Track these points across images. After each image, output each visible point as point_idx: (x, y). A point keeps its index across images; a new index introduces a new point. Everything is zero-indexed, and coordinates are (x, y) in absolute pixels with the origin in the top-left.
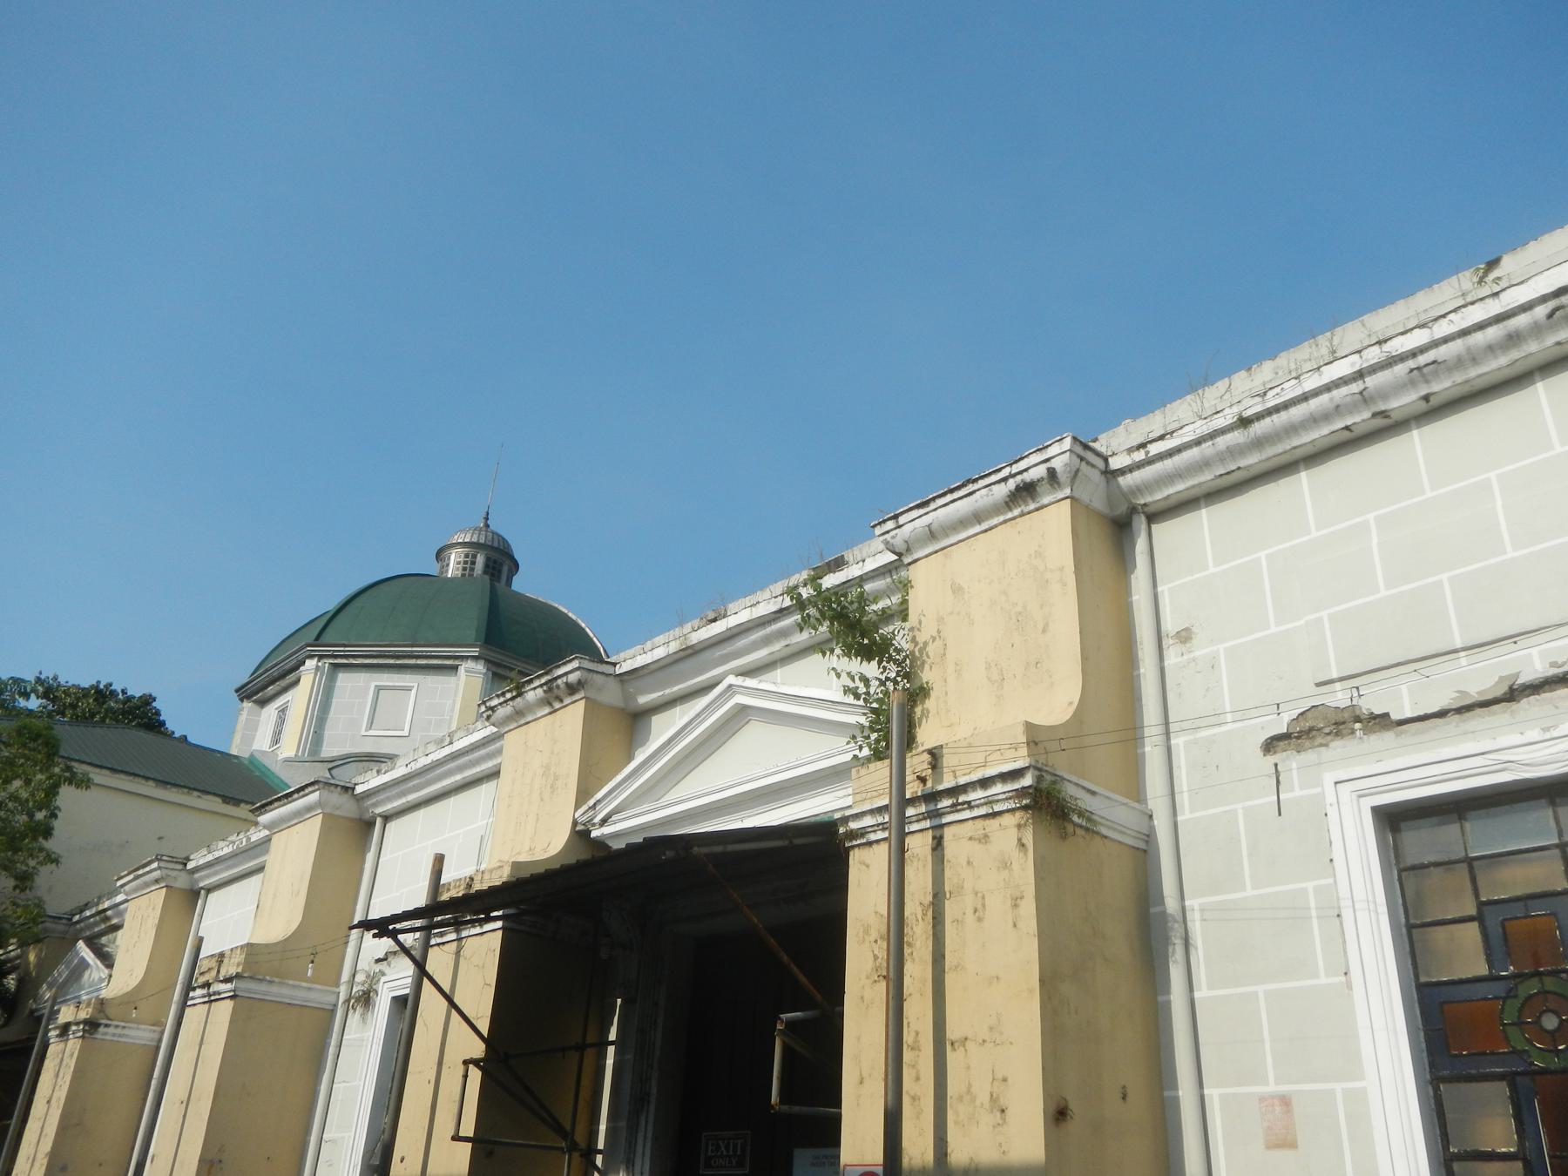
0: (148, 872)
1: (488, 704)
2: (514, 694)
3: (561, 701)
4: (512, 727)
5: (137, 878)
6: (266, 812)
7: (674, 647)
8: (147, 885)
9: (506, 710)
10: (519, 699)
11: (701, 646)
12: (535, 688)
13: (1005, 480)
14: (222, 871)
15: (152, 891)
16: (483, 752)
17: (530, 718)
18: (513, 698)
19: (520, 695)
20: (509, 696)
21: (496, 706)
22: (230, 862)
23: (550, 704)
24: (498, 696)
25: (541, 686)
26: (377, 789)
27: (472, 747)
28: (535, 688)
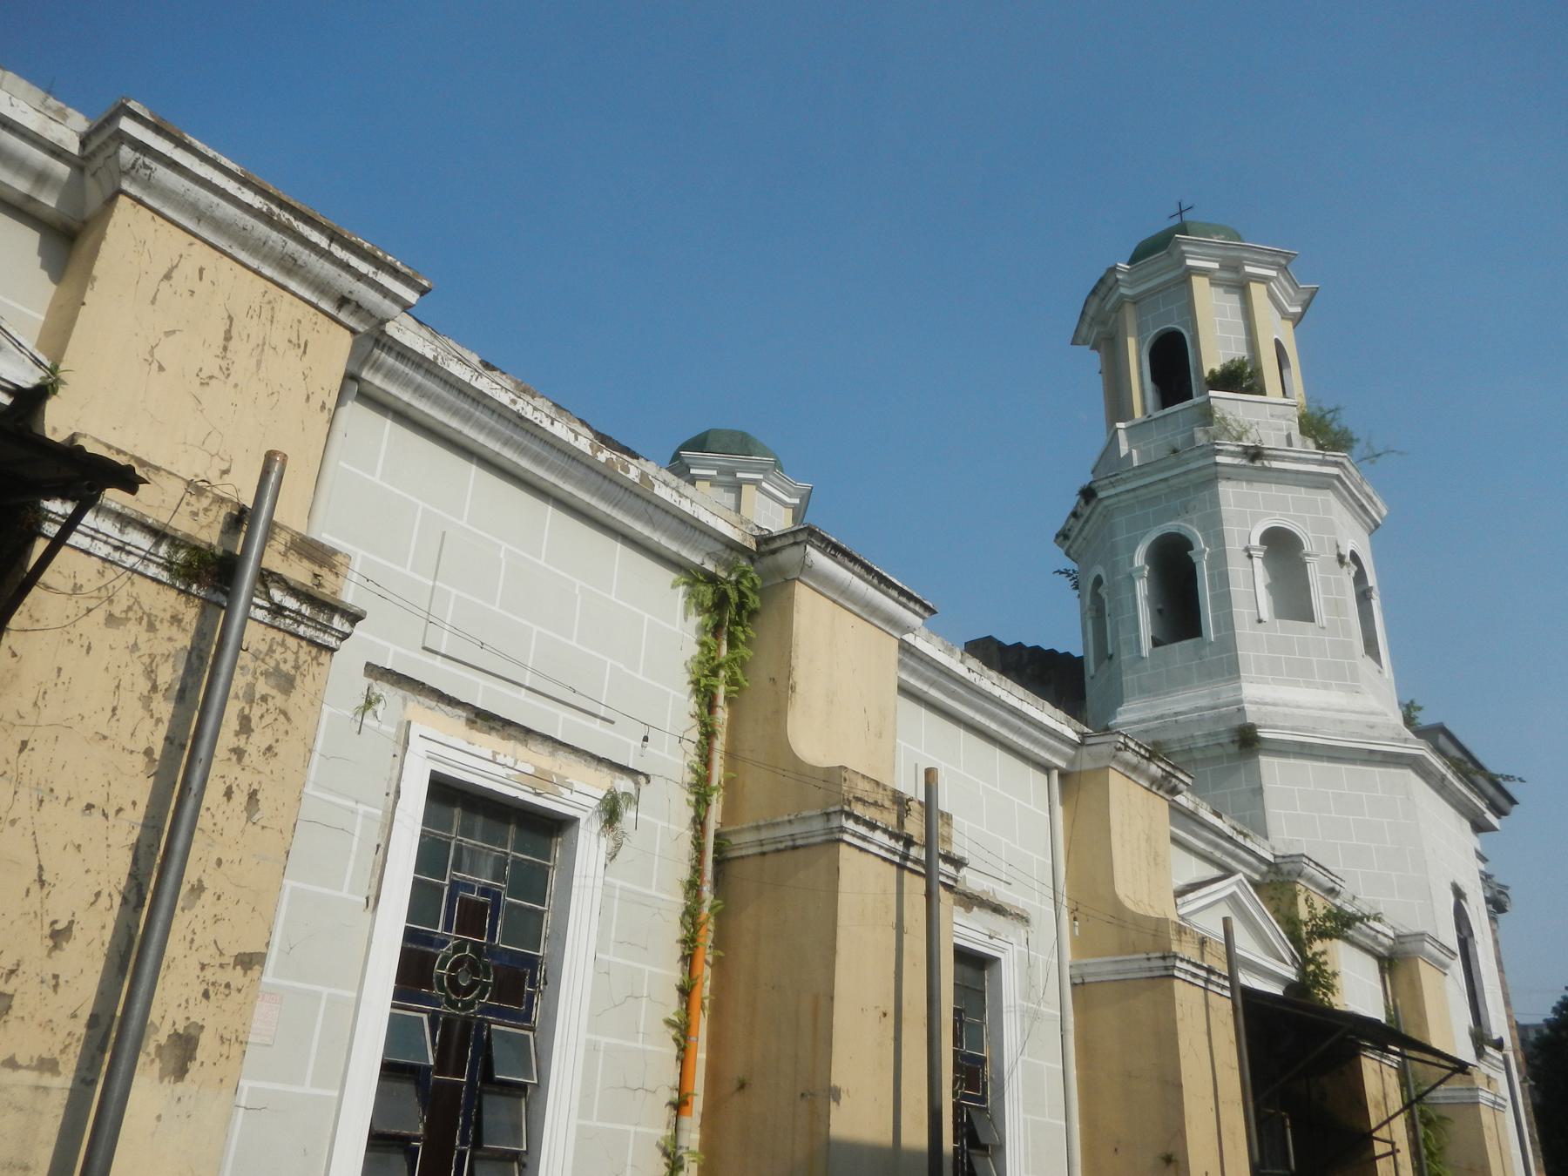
0: (361, 277)
1: (1127, 740)
2: (1147, 755)
3: (1158, 789)
4: (1119, 769)
5: (267, 218)
6: (833, 557)
7: (1191, 806)
8: (290, 266)
9: (1134, 759)
10: (1145, 761)
11: (1199, 819)
12: (1159, 767)
13: (1332, 880)
14: (481, 427)
15: (284, 288)
16: (1037, 734)
17: (1133, 777)
18: (1143, 756)
19: (1149, 759)
20: (1143, 752)
21: (1129, 748)
22: (536, 447)
23: (1152, 784)
24: (1137, 744)
25: (1163, 770)
26: (923, 656)
27: (946, 671)
28: (1159, 767)
